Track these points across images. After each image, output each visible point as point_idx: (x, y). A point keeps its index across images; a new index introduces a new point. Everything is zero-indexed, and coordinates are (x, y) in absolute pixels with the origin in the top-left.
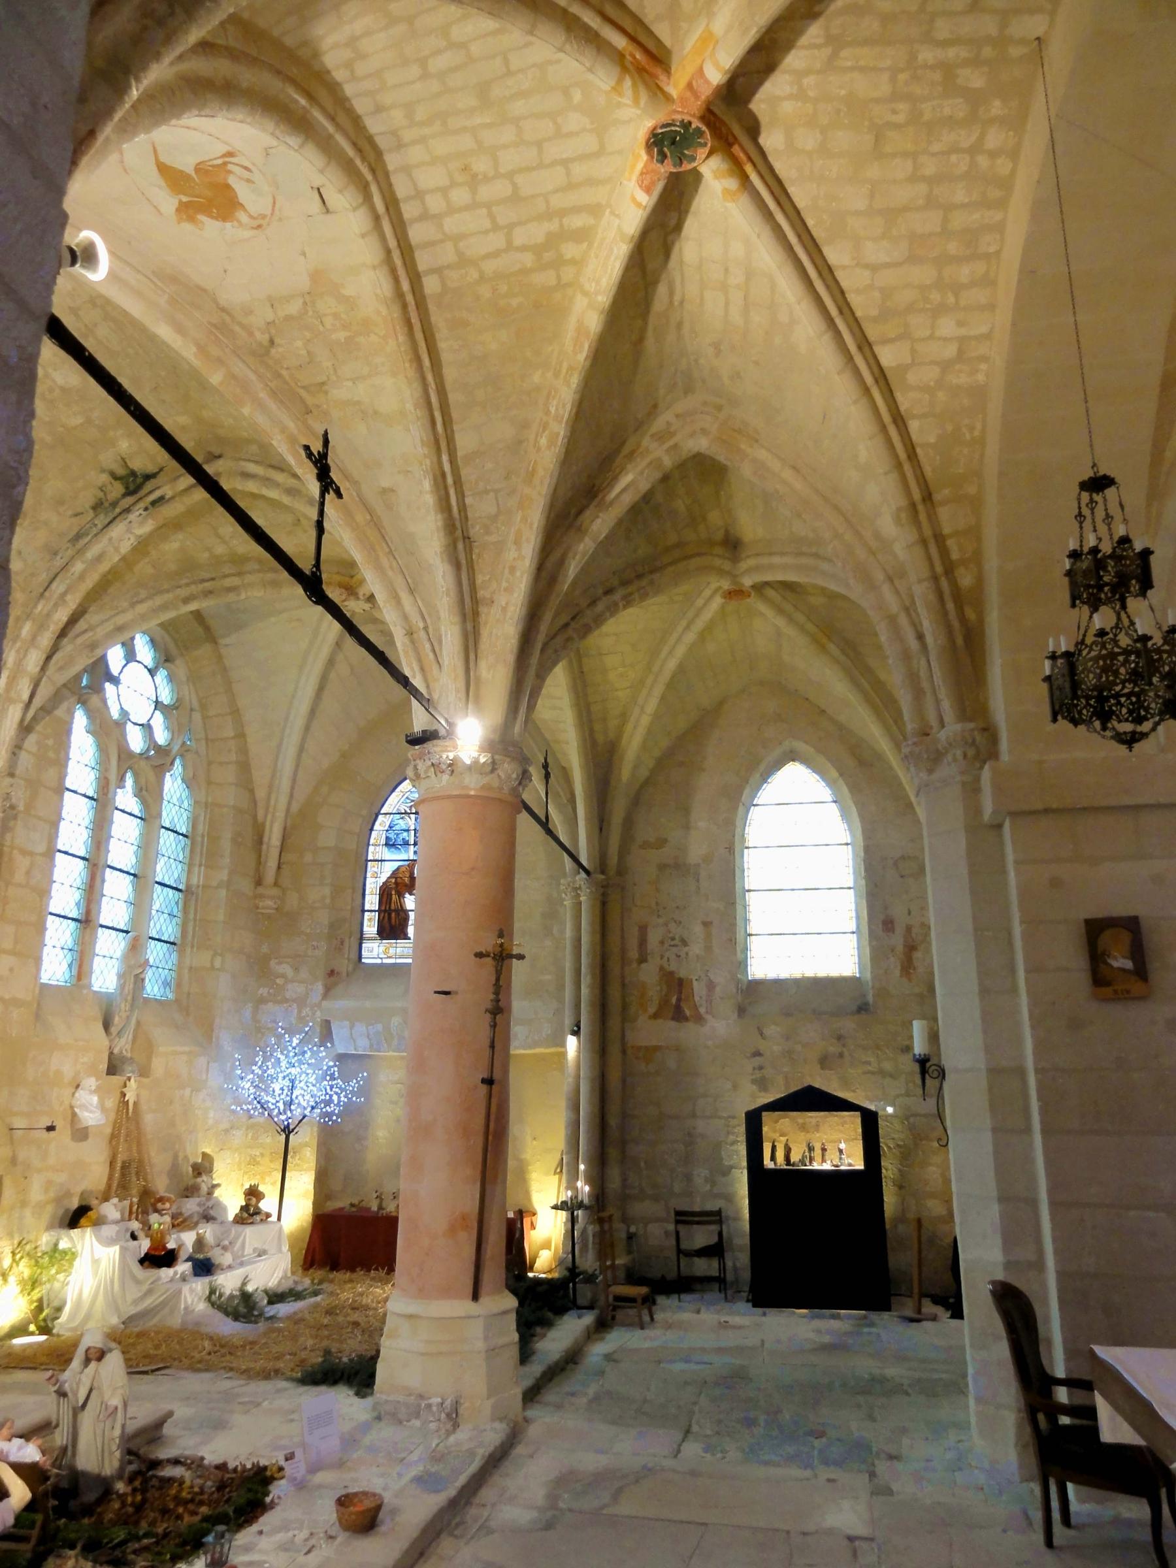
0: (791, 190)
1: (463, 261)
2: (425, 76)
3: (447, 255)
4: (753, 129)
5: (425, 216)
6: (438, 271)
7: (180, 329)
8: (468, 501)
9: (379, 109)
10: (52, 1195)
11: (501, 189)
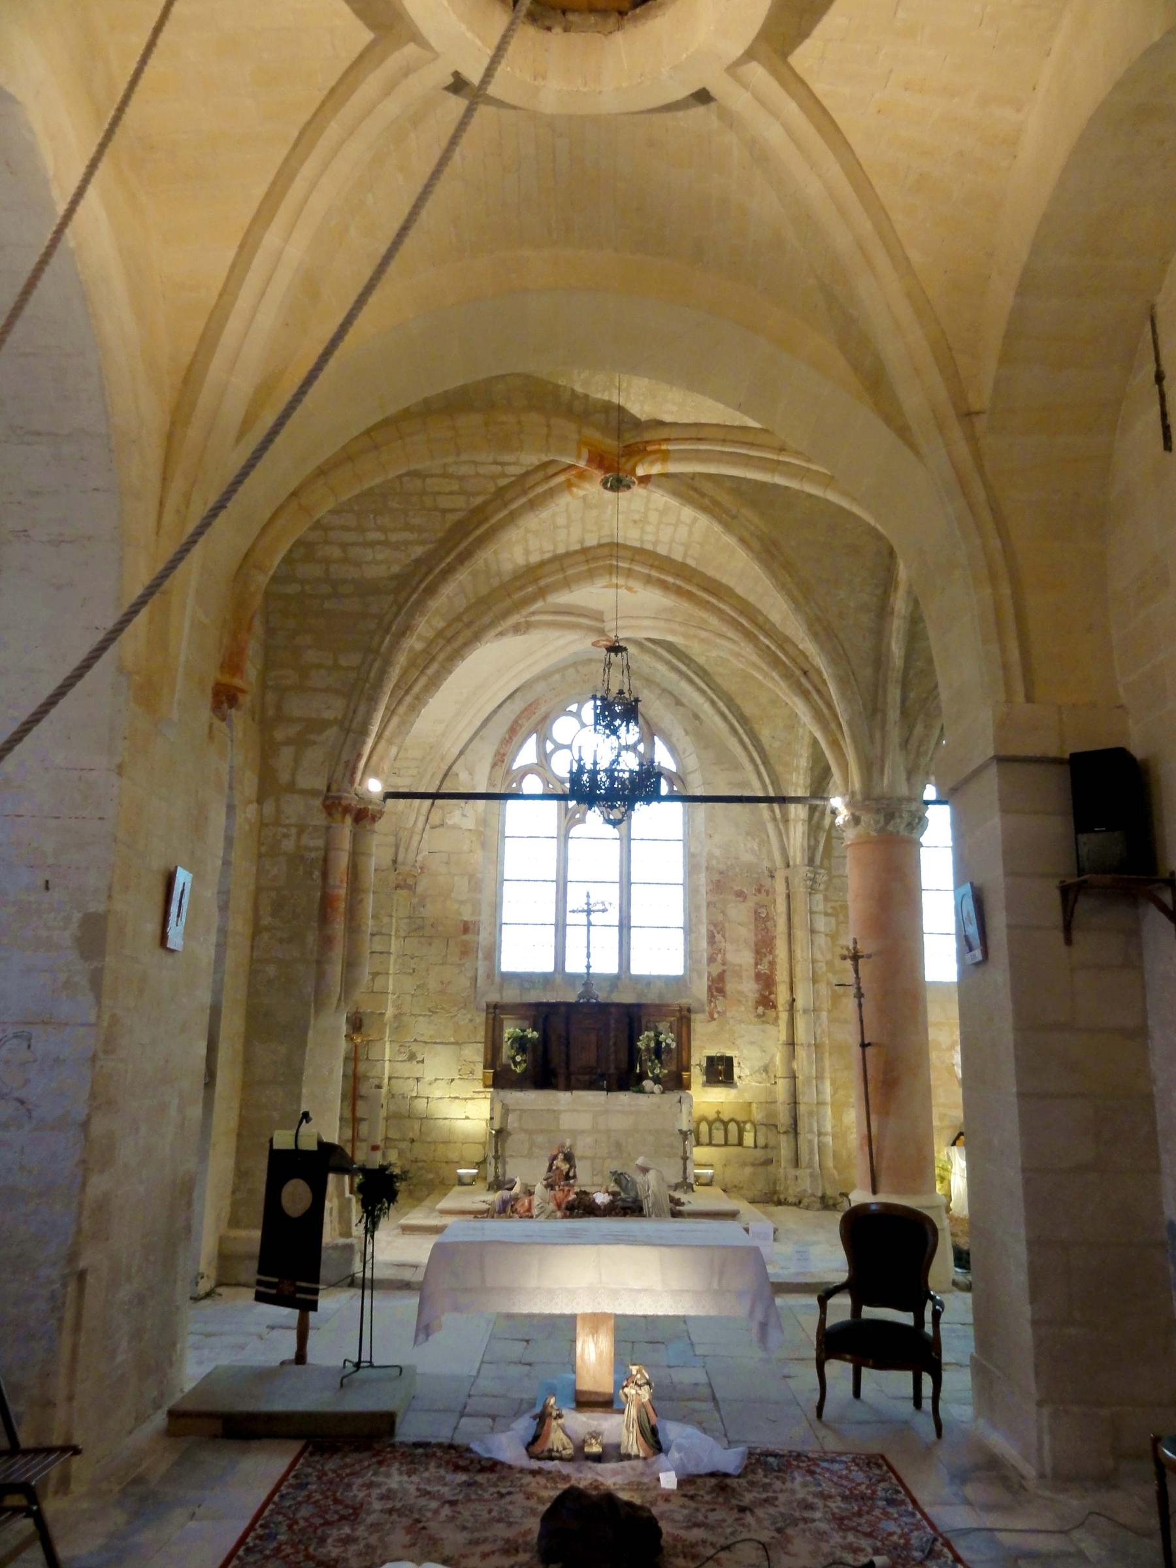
0: (703, 421)
1: (687, 546)
2: (567, 527)
3: (681, 549)
4: (661, 424)
5: (655, 543)
6: (685, 556)
7: (673, 632)
8: (801, 647)
9: (582, 541)
10: (947, 1123)
11: (653, 517)
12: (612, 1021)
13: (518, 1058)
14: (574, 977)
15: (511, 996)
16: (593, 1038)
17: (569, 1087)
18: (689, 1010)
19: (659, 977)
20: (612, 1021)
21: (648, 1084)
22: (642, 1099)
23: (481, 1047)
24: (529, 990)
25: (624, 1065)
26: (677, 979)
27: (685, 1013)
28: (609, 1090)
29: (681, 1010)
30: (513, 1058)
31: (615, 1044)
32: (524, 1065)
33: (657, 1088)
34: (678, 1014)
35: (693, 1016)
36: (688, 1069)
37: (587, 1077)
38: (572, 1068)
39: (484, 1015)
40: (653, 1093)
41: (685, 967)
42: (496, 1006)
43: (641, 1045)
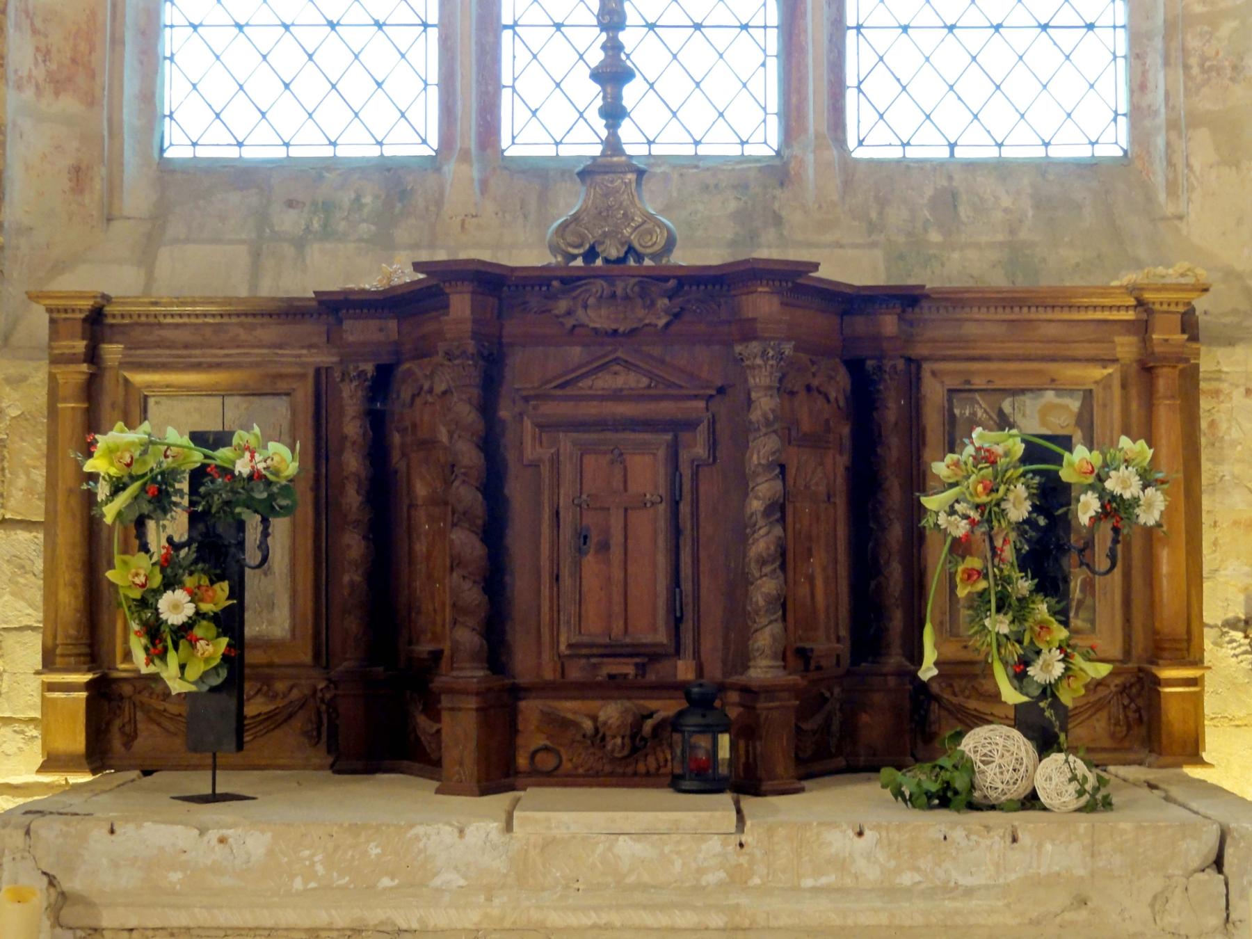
12: (761, 378)
13: (175, 607)
14: (540, 174)
15: (201, 270)
16: (646, 472)
17: (499, 773)
18: (1189, 324)
19: (1002, 169)
20: (761, 378)
21: (994, 751)
22: (969, 850)
23: (29, 543)
24: (300, 244)
25: (830, 644)
26: (1091, 168)
27: (1166, 335)
28: (747, 782)
29: (1142, 328)
30: (146, 602)
31: (778, 510)
32: (212, 648)
33: (1055, 776)
34: (1126, 348)
35: (1210, 360)
36: (1185, 649)
37: (612, 712)
38: (528, 661)
39: (39, 374)
40: (1031, 801)
41: (1137, 114)
42: (97, 322)
43: (944, 511)
